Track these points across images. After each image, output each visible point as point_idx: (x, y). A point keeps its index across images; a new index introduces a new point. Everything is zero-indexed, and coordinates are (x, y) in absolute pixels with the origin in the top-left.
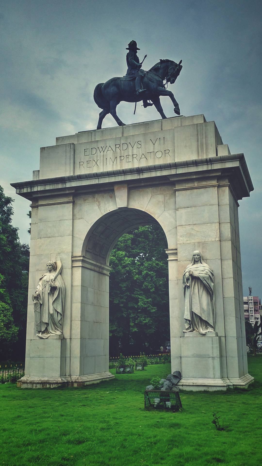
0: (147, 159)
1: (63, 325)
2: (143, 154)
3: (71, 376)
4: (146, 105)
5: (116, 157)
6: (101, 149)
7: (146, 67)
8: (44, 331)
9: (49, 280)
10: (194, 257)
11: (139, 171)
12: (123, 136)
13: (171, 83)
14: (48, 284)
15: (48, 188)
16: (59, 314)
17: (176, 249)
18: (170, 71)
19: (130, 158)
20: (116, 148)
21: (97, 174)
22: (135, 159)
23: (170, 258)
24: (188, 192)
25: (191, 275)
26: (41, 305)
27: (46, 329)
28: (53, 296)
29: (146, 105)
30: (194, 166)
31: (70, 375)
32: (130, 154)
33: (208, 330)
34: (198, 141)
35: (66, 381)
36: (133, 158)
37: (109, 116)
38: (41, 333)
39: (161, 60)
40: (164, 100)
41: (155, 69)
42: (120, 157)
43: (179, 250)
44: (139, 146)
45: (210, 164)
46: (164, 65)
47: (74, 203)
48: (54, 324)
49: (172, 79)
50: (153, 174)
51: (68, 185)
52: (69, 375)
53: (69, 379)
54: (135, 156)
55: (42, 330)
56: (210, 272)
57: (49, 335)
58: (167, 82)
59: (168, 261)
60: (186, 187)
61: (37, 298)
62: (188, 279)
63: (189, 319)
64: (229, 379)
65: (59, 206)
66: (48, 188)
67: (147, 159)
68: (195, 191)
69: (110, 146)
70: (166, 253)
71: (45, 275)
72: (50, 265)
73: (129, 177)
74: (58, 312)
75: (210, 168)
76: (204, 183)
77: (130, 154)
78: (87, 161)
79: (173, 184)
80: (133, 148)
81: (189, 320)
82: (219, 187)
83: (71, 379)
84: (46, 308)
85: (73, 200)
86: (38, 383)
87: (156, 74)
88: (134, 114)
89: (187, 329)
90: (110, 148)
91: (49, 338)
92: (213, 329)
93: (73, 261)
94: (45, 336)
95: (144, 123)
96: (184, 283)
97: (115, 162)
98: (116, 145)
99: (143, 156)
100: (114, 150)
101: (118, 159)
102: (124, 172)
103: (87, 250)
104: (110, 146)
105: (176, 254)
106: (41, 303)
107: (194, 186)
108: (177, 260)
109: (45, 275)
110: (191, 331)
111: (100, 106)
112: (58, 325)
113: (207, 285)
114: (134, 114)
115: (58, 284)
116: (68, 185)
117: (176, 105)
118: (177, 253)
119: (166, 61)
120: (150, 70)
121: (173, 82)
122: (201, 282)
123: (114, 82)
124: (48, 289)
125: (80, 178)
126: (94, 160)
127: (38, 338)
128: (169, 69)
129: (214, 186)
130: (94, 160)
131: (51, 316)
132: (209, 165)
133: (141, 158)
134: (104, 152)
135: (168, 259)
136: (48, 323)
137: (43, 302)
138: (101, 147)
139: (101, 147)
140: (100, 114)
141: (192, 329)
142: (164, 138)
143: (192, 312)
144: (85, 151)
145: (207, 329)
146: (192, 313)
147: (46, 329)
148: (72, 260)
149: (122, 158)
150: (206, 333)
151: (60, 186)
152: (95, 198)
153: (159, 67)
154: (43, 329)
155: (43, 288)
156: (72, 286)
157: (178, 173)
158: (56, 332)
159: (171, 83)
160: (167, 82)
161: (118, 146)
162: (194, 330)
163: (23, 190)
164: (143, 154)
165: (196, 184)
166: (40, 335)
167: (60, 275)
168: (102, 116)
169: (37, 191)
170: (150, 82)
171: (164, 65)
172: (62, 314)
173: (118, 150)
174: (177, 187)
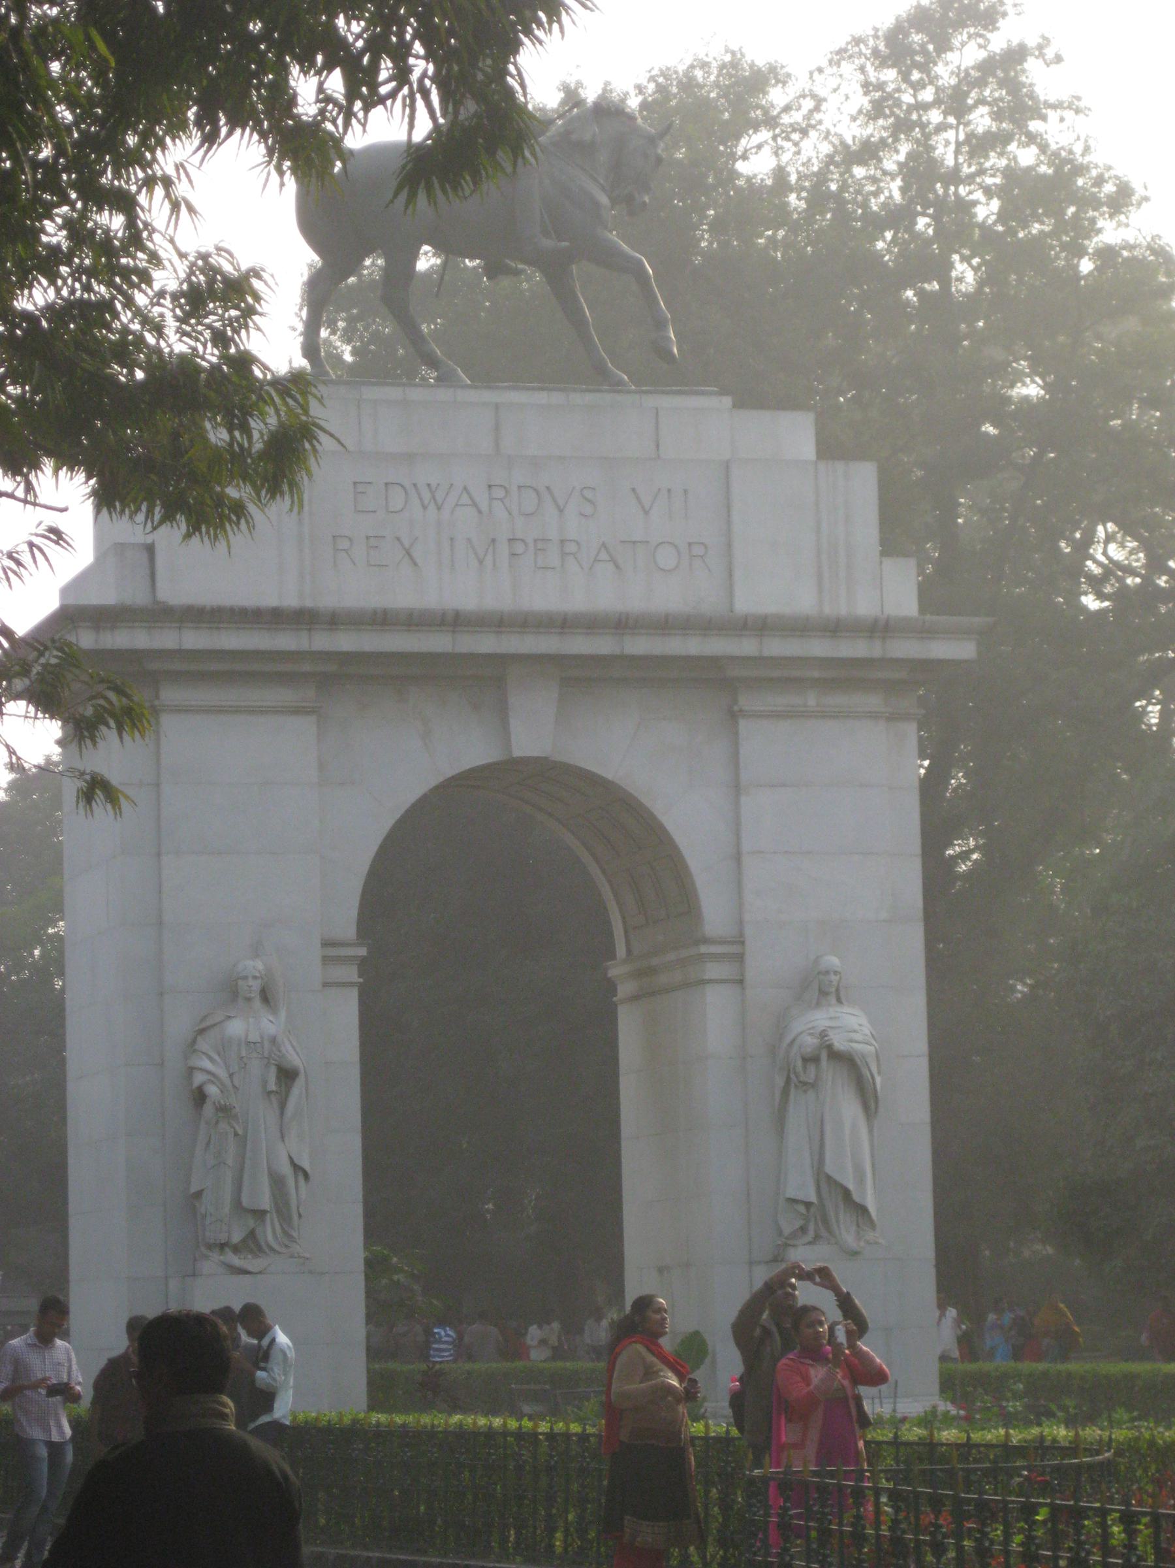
0: (617, 566)
5: (493, 541)
6: (427, 496)
9: (262, 1037)
10: (821, 977)
17: (743, 943)
20: (491, 499)
27: (252, 1234)
36: (564, 555)
42: (510, 540)
50: (675, 646)
54: (571, 548)
55: (236, 1238)
67: (617, 566)
69: (465, 488)
72: (258, 975)
73: (579, 645)
80: (561, 511)
90: (465, 499)
93: (326, 960)
97: (489, 558)
98: (490, 486)
99: (604, 556)
100: (484, 507)
101: (503, 549)
110: (810, 1243)
113: (871, 1081)
129: (874, 716)
131: (277, 1182)
133: (595, 560)
139: (429, 485)
146: (825, 1181)
149: (519, 548)
157: (766, 653)
161: (499, 493)
164: (604, 545)
165: (811, 700)
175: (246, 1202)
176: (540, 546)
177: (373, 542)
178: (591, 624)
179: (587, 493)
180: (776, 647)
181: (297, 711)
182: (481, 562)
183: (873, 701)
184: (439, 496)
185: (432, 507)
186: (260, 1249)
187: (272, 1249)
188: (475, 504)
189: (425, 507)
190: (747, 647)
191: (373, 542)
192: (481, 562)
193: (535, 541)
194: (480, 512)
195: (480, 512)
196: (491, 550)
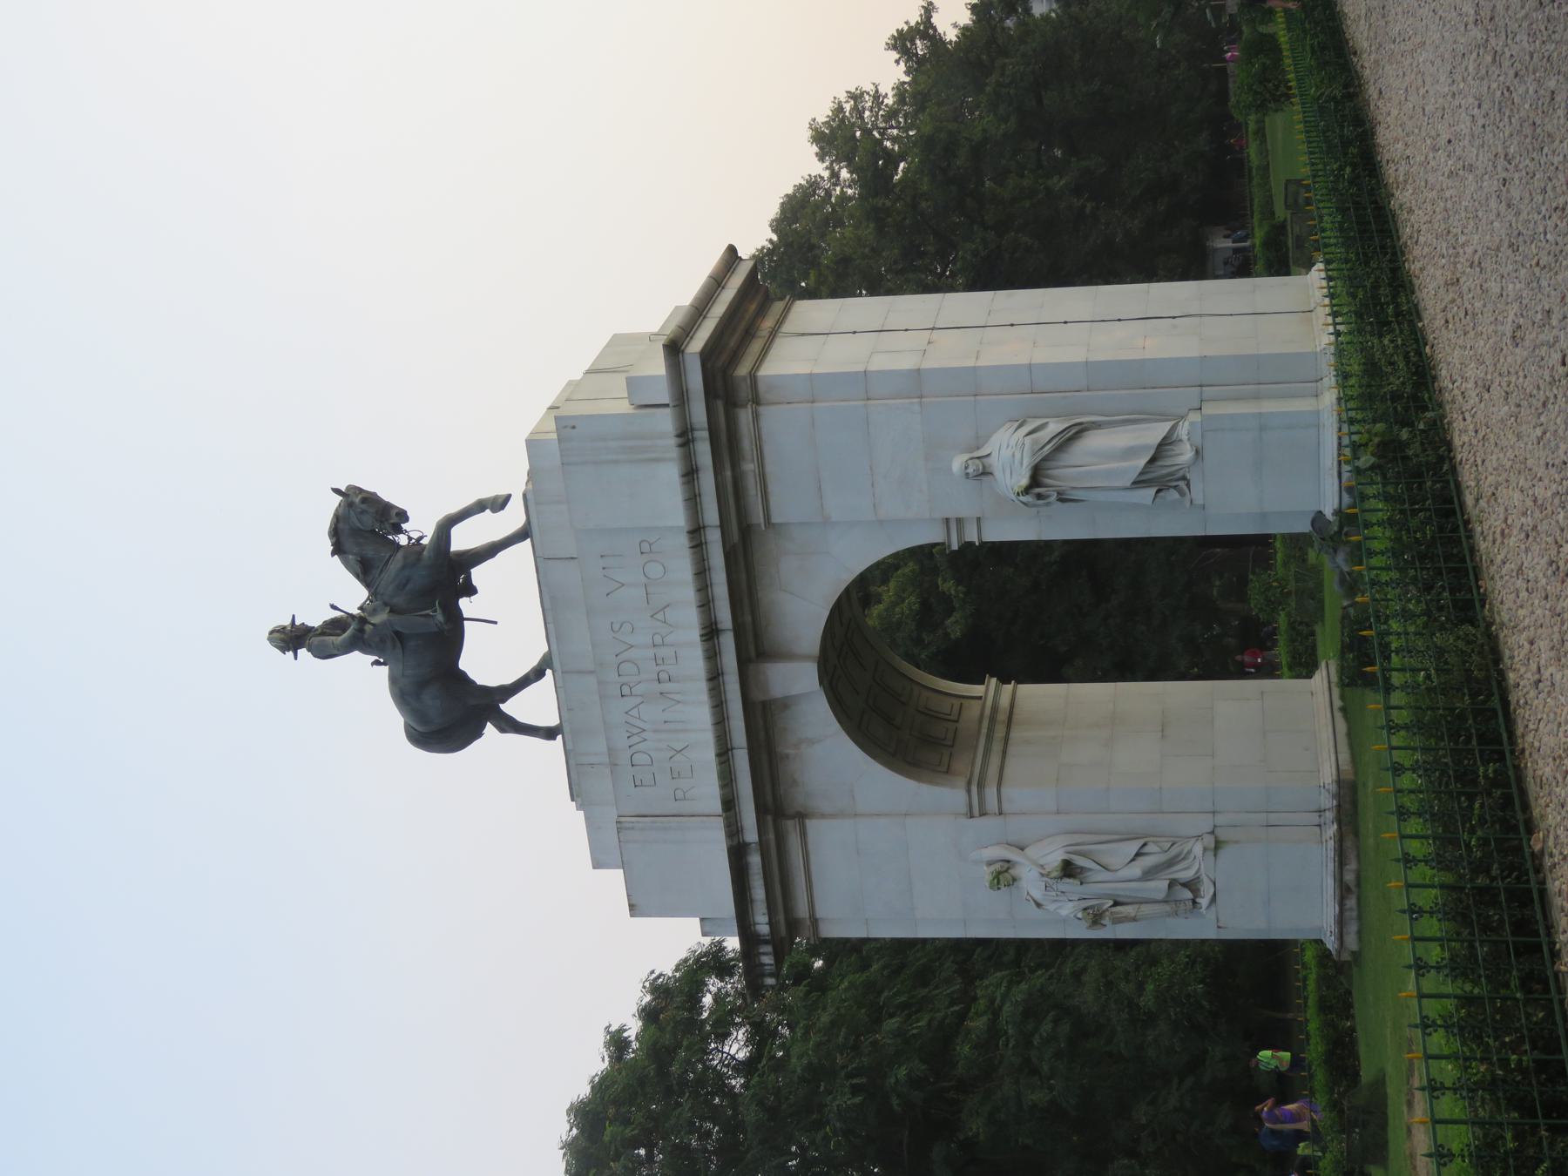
1: (1177, 837)
2: (652, 616)
3: (1320, 807)
4: (470, 590)
5: (661, 693)
6: (635, 739)
7: (352, 595)
8: (1192, 891)
11: (711, 632)
12: (592, 672)
13: (406, 519)
14: (1054, 887)
15: (758, 892)
16: (1146, 850)
17: (947, 520)
18: (368, 521)
19: (662, 652)
21: (718, 755)
22: (669, 639)
23: (972, 536)
24: (773, 488)
25: (1027, 491)
26: (1116, 904)
28: (1090, 870)
29: (470, 590)
30: (698, 478)
31: (1320, 811)
32: (650, 653)
33: (1185, 438)
34: (616, 462)
35: (1335, 826)
37: (508, 707)
38: (1198, 900)
39: (333, 553)
40: (463, 539)
41: (364, 571)
43: (951, 514)
44: (627, 627)
45: (692, 434)
46: (348, 544)
47: (802, 816)
48: (1171, 863)
49: (394, 520)
51: (751, 835)
52: (1318, 814)
53: (1330, 815)
54: (658, 640)
55: (1189, 895)
56: (1016, 430)
57: (1205, 880)
58: (399, 531)
59: (983, 544)
60: (757, 495)
61: (1096, 919)
62: (1039, 497)
63: (1153, 491)
64: (1321, 379)
65: (813, 858)
66: (758, 892)
68: (769, 468)
69: (627, 713)
70: (959, 548)
71: (1028, 893)
72: (996, 881)
74: (1138, 854)
75: (706, 434)
76: (747, 444)
77: (650, 653)
78: (673, 778)
79: (746, 530)
80: (632, 646)
81: (1158, 491)
82: (756, 401)
83: (1329, 809)
84: (1121, 889)
85: (797, 820)
86: (1341, 905)
87: (379, 570)
88: (496, 623)
89: (1182, 494)
90: (634, 713)
91: (1213, 878)
92: (1181, 423)
93: (983, 814)
94: (1207, 890)
95: (547, 606)
96: (1048, 504)
97: (677, 697)
98: (622, 696)
99: (660, 616)
100: (639, 700)
101: (667, 687)
102: (715, 677)
103: (945, 769)
104: (627, 713)
105: (959, 521)
106: (1111, 903)
107: (754, 471)
108: (979, 519)
109: (1028, 893)
110: (1188, 485)
111: (477, 733)
112: (1174, 851)
113: (1054, 441)
114: (496, 623)
115: (1054, 858)
116: (751, 835)
117: (480, 507)
118: (957, 519)
119: (334, 540)
120: (368, 585)
121: (403, 516)
122: (1045, 459)
123: (405, 695)
124: (1069, 885)
125: (730, 803)
126: (671, 758)
127: (1213, 908)
128: (362, 527)
129: (756, 417)
130: (671, 758)
131: (1148, 874)
132: (694, 436)
134: (644, 730)
135: (977, 544)
136: (1168, 882)
137: (1107, 896)
138: (628, 737)
139: (628, 737)
140: (502, 730)
141: (1182, 484)
142: (602, 556)
143: (1134, 483)
144: (642, 786)
145: (1181, 440)
146: (1139, 483)
147: (1186, 885)
148: (980, 816)
149: (663, 676)
150: (1191, 445)
151: (755, 860)
152: (787, 756)
153: (359, 559)
154: (1188, 895)
155: (1065, 898)
156: (1058, 813)
157: (717, 522)
158: (1195, 857)
159: (406, 519)
160: (399, 531)
161: (626, 690)
162: (1184, 478)
163: (768, 965)
165: (749, 467)
166: (1204, 902)
167: (1026, 850)
168: (510, 725)
169: (770, 923)
170: (409, 587)
171: (348, 544)
172: (1142, 842)
173: (637, 690)
174: (758, 517)
175: (1161, 896)
176: (660, 662)
177: (675, 775)
178: (712, 655)
179: (616, 627)
180: (711, 515)
181: (803, 834)
182: (679, 702)
183: (744, 416)
184: (636, 731)
185: (644, 735)
186: (1198, 878)
187: (1197, 873)
188: (638, 705)
189: (645, 740)
190: (714, 537)
191: (675, 775)
192: (679, 702)
193: (657, 665)
194: (643, 702)
195: (643, 702)
196: (668, 695)
